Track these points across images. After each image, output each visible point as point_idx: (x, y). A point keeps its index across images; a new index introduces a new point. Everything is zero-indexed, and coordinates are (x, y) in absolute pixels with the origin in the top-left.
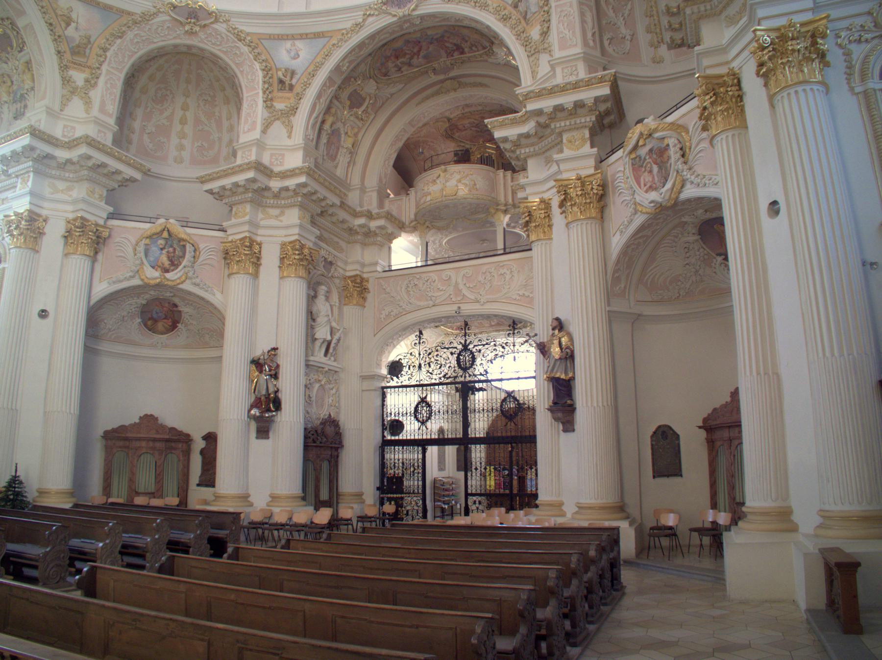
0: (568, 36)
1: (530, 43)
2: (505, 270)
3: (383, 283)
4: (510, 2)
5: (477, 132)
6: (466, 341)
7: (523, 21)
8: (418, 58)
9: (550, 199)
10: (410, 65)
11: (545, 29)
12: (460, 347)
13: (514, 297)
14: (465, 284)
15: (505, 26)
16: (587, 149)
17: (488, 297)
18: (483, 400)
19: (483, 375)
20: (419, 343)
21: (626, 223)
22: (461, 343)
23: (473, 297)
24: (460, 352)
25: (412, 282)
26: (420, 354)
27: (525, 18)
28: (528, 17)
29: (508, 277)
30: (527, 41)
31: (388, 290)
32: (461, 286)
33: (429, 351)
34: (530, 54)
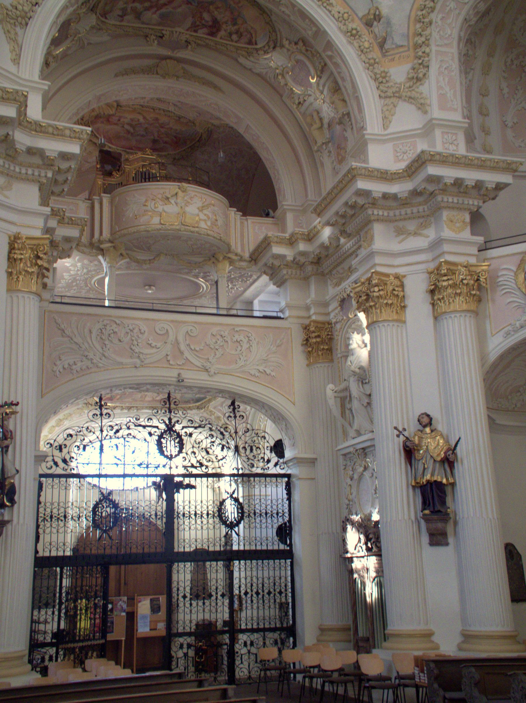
0: (448, 95)
1: (387, 81)
2: (242, 337)
3: (59, 321)
4: (361, 15)
5: (128, 132)
6: (170, 419)
7: (376, 48)
8: (155, 13)
9: (404, 276)
10: (138, 15)
11: (421, 75)
12: (163, 427)
13: (252, 372)
14: (189, 345)
15: (350, 43)
16: (466, 234)
17: (219, 366)
18: (196, 501)
19: (196, 467)
20: (101, 415)
21: (518, 324)
22: (164, 422)
23: (199, 364)
24: (162, 434)
25: (108, 327)
26: (102, 431)
27: (381, 45)
28: (387, 46)
29: (245, 346)
30: (384, 78)
31: (68, 332)
32: (183, 347)
33: (116, 428)
34: (383, 95)
